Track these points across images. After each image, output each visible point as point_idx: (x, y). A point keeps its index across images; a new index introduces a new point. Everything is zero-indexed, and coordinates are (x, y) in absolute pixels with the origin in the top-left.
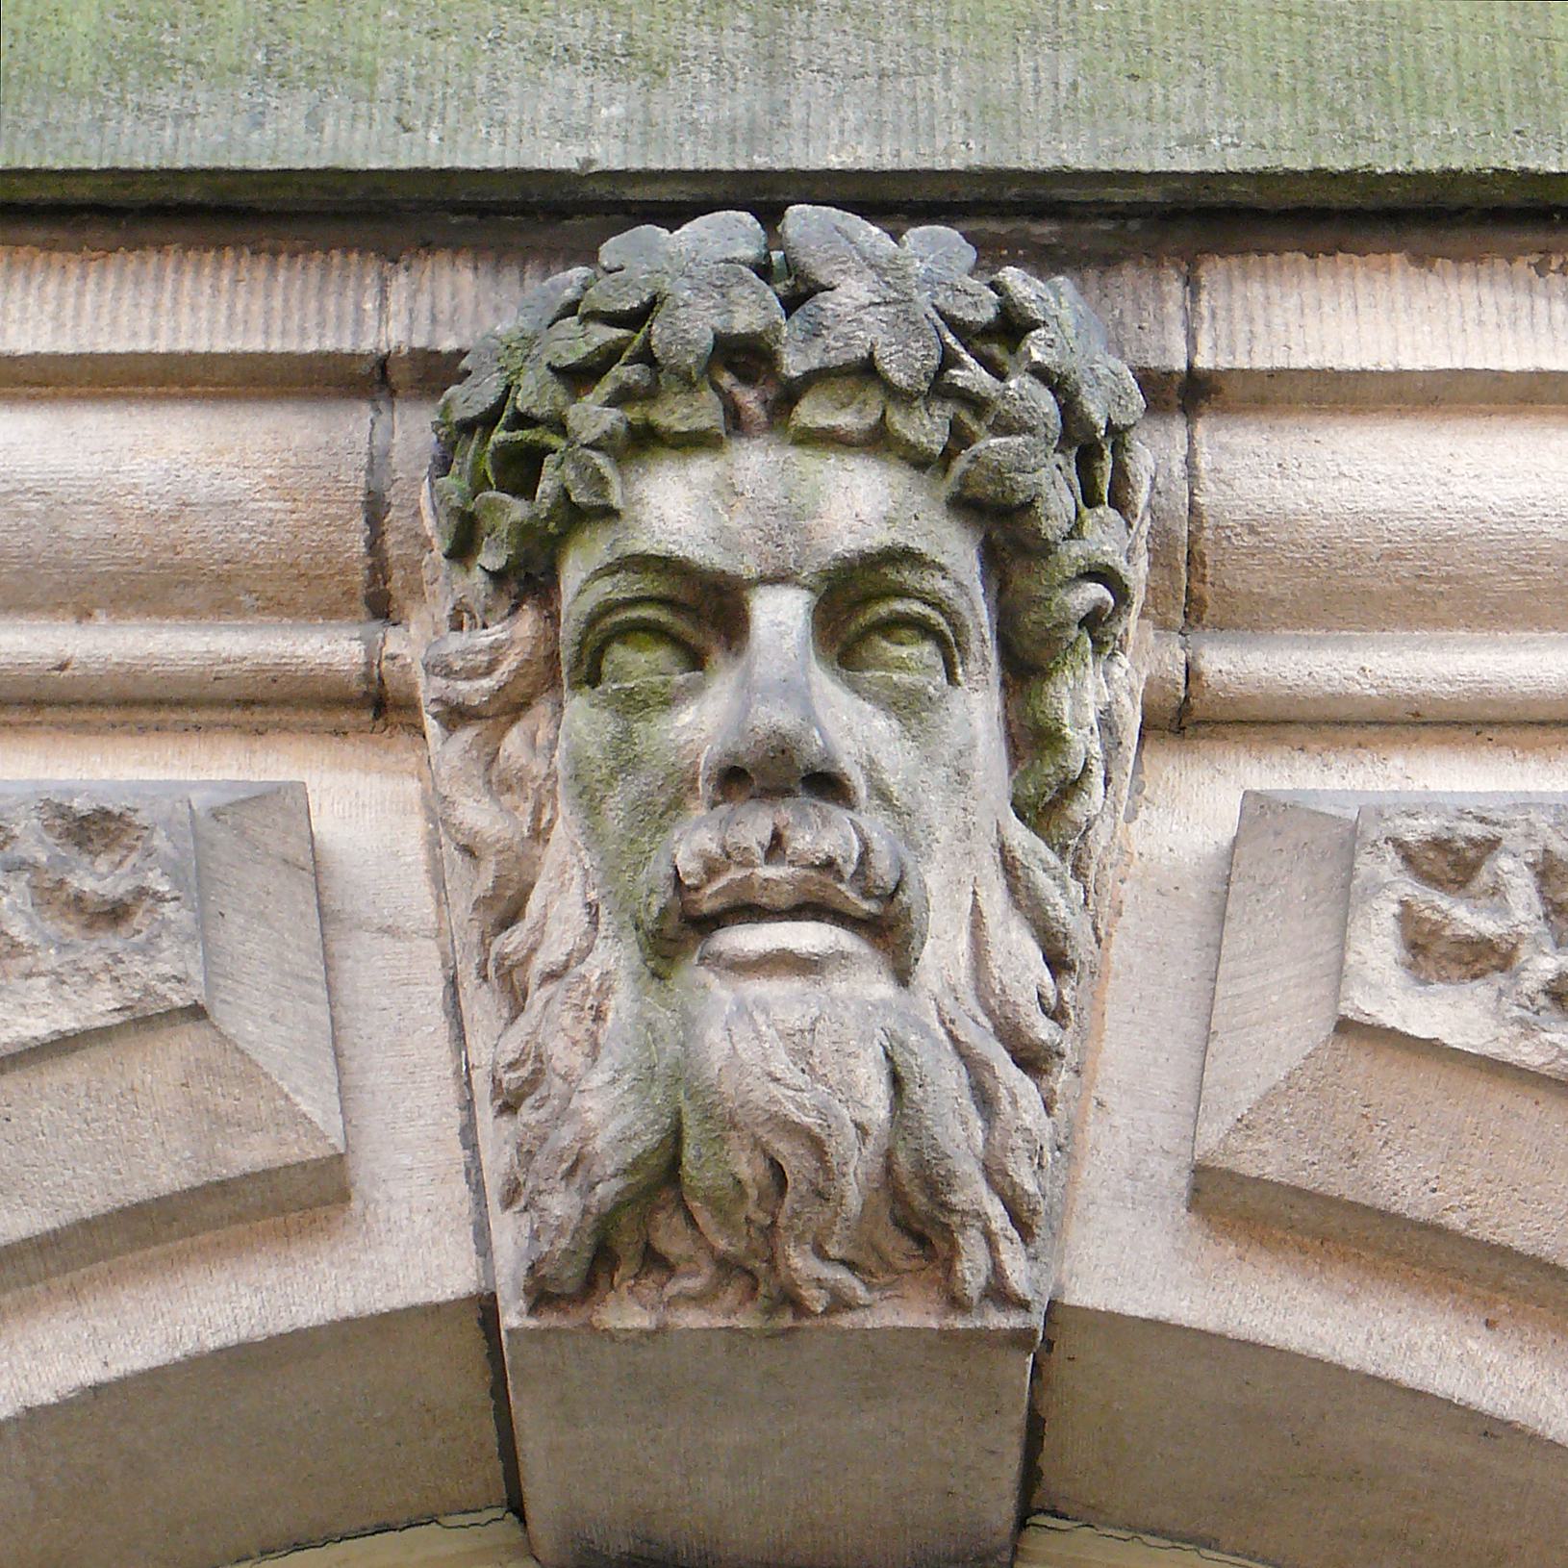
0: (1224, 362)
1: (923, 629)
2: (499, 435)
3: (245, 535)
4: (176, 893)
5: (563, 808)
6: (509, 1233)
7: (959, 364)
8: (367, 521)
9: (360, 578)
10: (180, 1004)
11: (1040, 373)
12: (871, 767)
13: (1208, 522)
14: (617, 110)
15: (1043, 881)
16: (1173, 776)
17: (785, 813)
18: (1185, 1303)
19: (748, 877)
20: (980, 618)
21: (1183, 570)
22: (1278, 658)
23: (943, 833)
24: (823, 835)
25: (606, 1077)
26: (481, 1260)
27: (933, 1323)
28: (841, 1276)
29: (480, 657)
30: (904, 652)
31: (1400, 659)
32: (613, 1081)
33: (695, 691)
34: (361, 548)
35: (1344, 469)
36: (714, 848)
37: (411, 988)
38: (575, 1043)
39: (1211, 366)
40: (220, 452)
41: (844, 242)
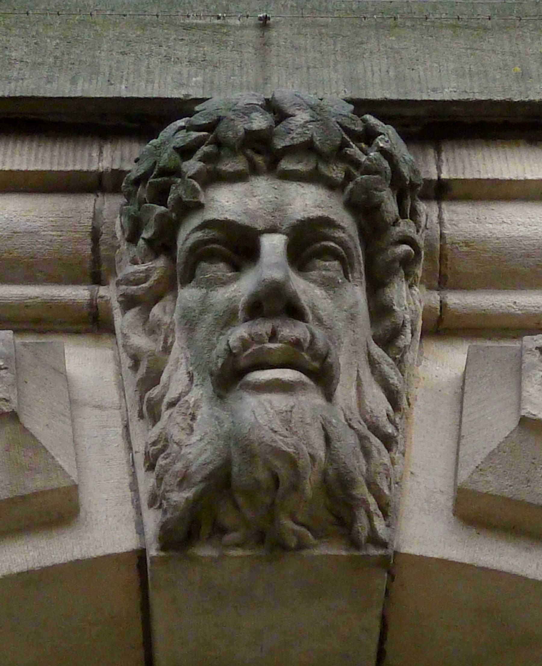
0: (453, 176)
1: (333, 255)
2: (151, 180)
3: (40, 246)
4: (6, 366)
5: (177, 335)
6: (152, 520)
7: (349, 146)
8: (92, 240)
9: (88, 265)
10: (6, 411)
11: (382, 151)
12: (313, 308)
13: (448, 241)
14: (199, 79)
15: (386, 368)
16: (435, 349)
17: (278, 322)
18: (454, 552)
19: (261, 348)
20: (359, 252)
21: (438, 262)
22: (479, 299)
23: (346, 340)
24: (292, 330)
25: (198, 438)
26: (138, 536)
27: (344, 553)
28: (303, 530)
29: (141, 275)
30: (327, 263)
31: (530, 299)
32: (201, 440)
33: (235, 279)
34: (89, 252)
35: (505, 220)
36: (246, 335)
37: (108, 429)
38: (183, 429)
39: (448, 177)
40: (30, 211)
41: (298, 99)
